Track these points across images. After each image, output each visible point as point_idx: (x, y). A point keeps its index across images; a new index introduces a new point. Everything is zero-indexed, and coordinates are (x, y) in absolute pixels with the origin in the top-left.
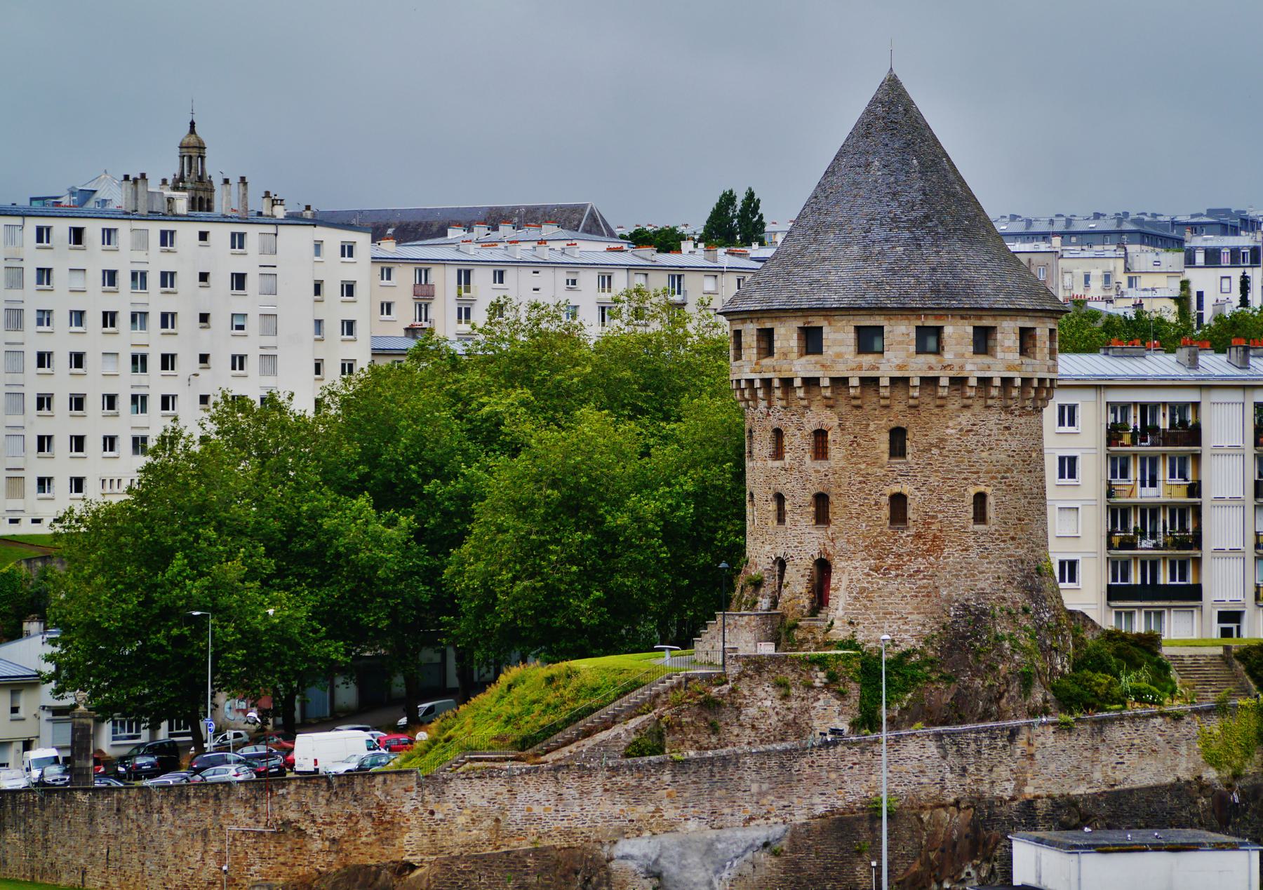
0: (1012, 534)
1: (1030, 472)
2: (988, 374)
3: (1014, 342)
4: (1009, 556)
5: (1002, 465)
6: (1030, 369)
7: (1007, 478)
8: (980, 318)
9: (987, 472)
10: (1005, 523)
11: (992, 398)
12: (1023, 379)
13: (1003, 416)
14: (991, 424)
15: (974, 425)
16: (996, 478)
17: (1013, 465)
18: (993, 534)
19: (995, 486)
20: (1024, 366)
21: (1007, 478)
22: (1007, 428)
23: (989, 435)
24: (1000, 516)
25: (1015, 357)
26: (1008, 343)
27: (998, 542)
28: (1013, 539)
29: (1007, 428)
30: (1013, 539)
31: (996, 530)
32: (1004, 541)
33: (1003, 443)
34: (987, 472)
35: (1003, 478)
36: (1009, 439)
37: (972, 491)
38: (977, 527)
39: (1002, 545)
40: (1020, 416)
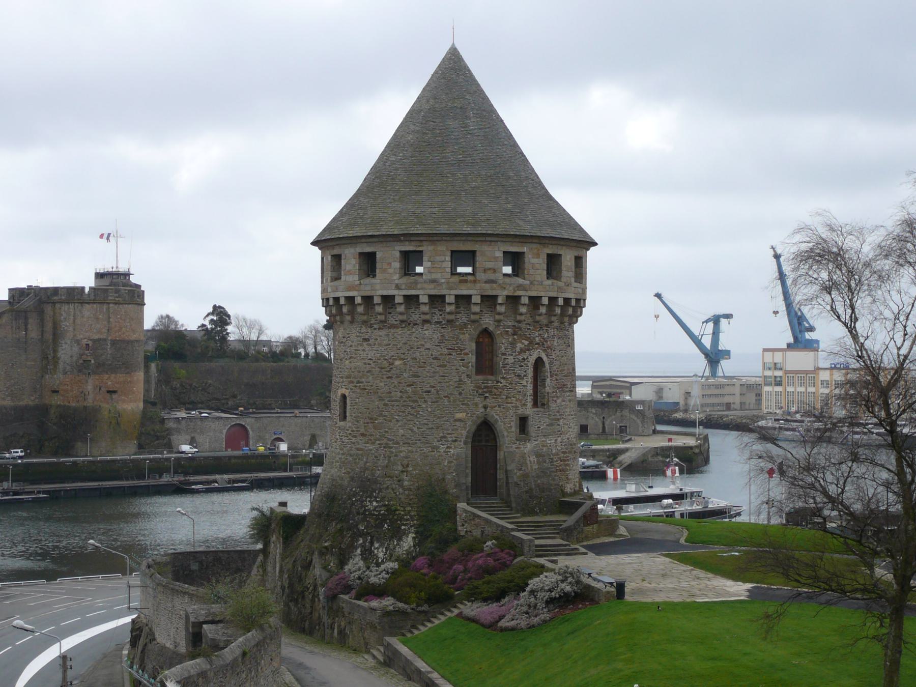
0: (362, 430)
1: (391, 377)
2: (337, 295)
3: (354, 265)
4: (358, 449)
5: (359, 372)
6: (368, 288)
7: (362, 382)
8: (333, 247)
9: (347, 377)
10: (357, 421)
11: (521, 314)
12: (363, 297)
13: (363, 330)
14: (353, 337)
15: (344, 337)
16: (352, 382)
17: (368, 372)
18: (348, 430)
19: (352, 389)
20: (362, 286)
21: (362, 382)
22: (365, 340)
23: (351, 346)
24: (354, 415)
25: (354, 279)
26: (349, 267)
27: (350, 437)
28: (363, 435)
29: (365, 340)
30: (363, 435)
31: (349, 427)
32: (355, 437)
33: (361, 352)
34: (347, 377)
35: (358, 382)
36: (367, 348)
37: (339, 394)
38: (342, 423)
39: (354, 440)
40: (379, 329)
